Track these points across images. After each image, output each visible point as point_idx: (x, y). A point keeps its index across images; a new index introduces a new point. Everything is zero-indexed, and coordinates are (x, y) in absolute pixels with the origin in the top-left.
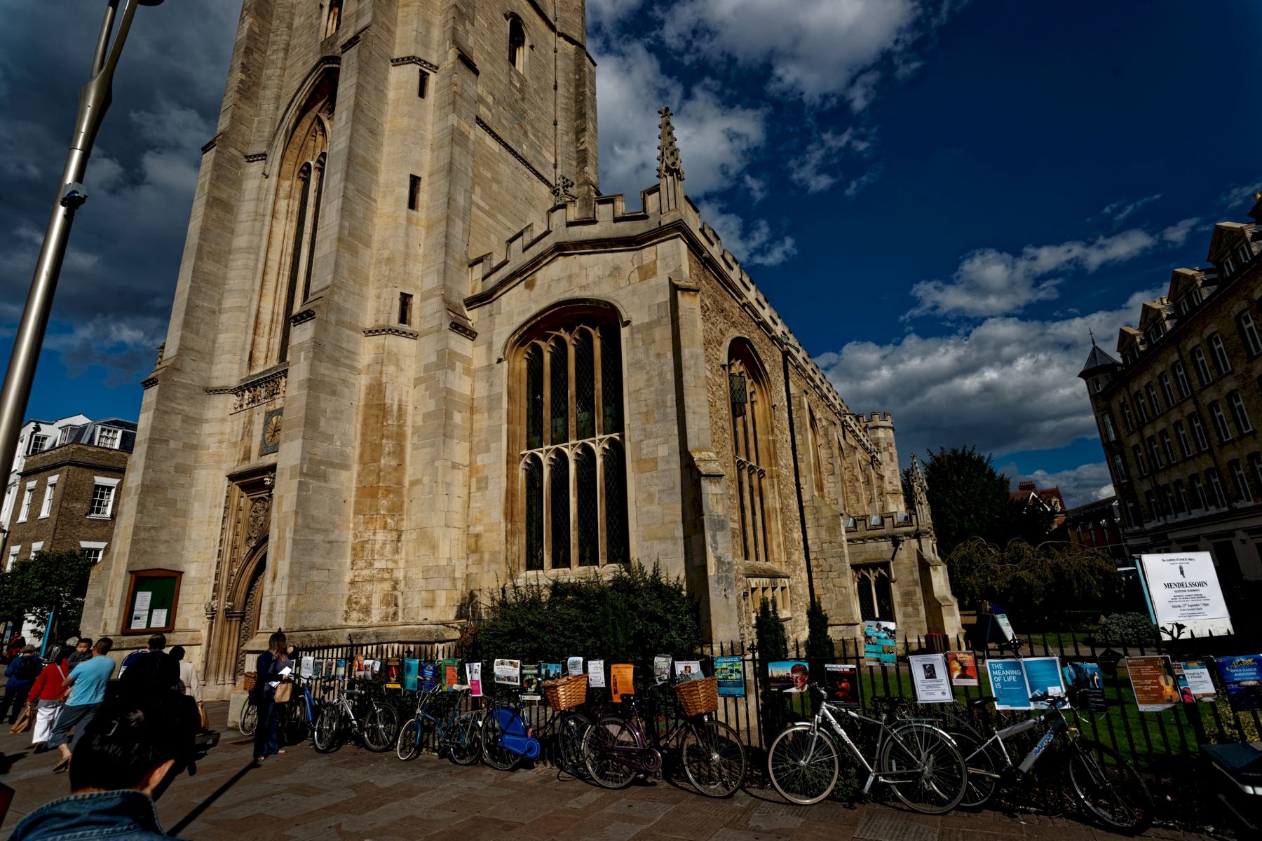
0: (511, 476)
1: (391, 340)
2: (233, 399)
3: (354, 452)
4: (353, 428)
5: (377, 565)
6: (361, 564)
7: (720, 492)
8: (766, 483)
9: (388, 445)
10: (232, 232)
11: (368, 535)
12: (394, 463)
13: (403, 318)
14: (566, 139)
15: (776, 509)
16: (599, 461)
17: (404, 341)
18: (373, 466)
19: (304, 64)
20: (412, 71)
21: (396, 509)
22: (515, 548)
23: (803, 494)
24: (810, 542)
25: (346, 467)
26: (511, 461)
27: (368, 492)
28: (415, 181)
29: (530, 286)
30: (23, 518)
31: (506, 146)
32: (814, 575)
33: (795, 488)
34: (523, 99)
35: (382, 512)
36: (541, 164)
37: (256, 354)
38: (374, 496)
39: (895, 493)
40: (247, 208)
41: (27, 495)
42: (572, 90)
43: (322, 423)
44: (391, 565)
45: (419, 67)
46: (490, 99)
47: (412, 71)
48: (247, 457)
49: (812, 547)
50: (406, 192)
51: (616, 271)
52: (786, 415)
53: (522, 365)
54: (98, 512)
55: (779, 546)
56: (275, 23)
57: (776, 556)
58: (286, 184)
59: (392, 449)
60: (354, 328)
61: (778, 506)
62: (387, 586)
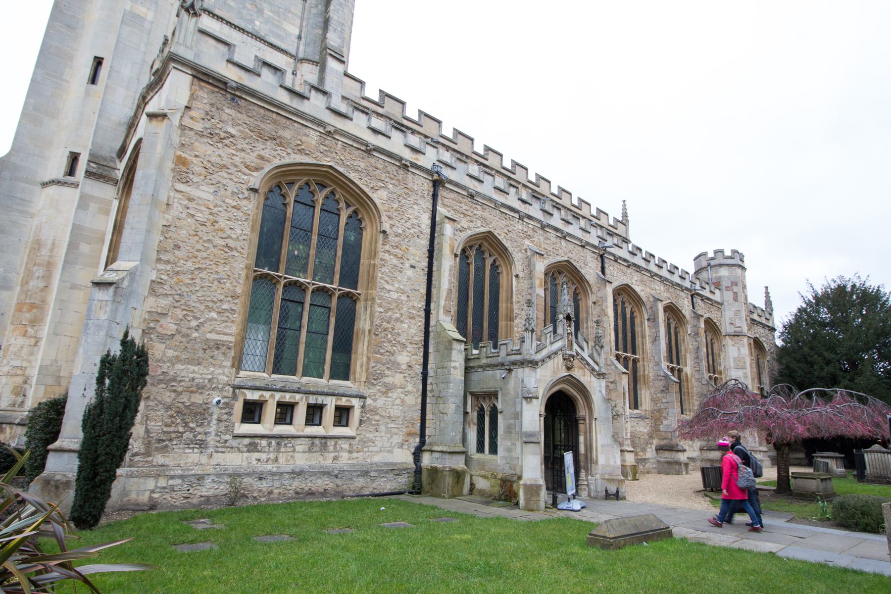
1: (53, 190)
4: (20, 259)
7: (106, 298)
8: (360, 306)
12: (41, 285)
13: (71, 171)
15: (364, 330)
21: (35, 322)
23: (431, 319)
24: (429, 367)
31: (228, 23)
32: (428, 400)
33: (423, 314)
35: (24, 323)
36: (278, 36)
39: (737, 335)
44: (25, 364)
49: (431, 372)
50: (87, 71)
52: (425, 242)
55: (361, 366)
57: (358, 376)
59: (41, 274)
61: (367, 327)
62: (19, 380)
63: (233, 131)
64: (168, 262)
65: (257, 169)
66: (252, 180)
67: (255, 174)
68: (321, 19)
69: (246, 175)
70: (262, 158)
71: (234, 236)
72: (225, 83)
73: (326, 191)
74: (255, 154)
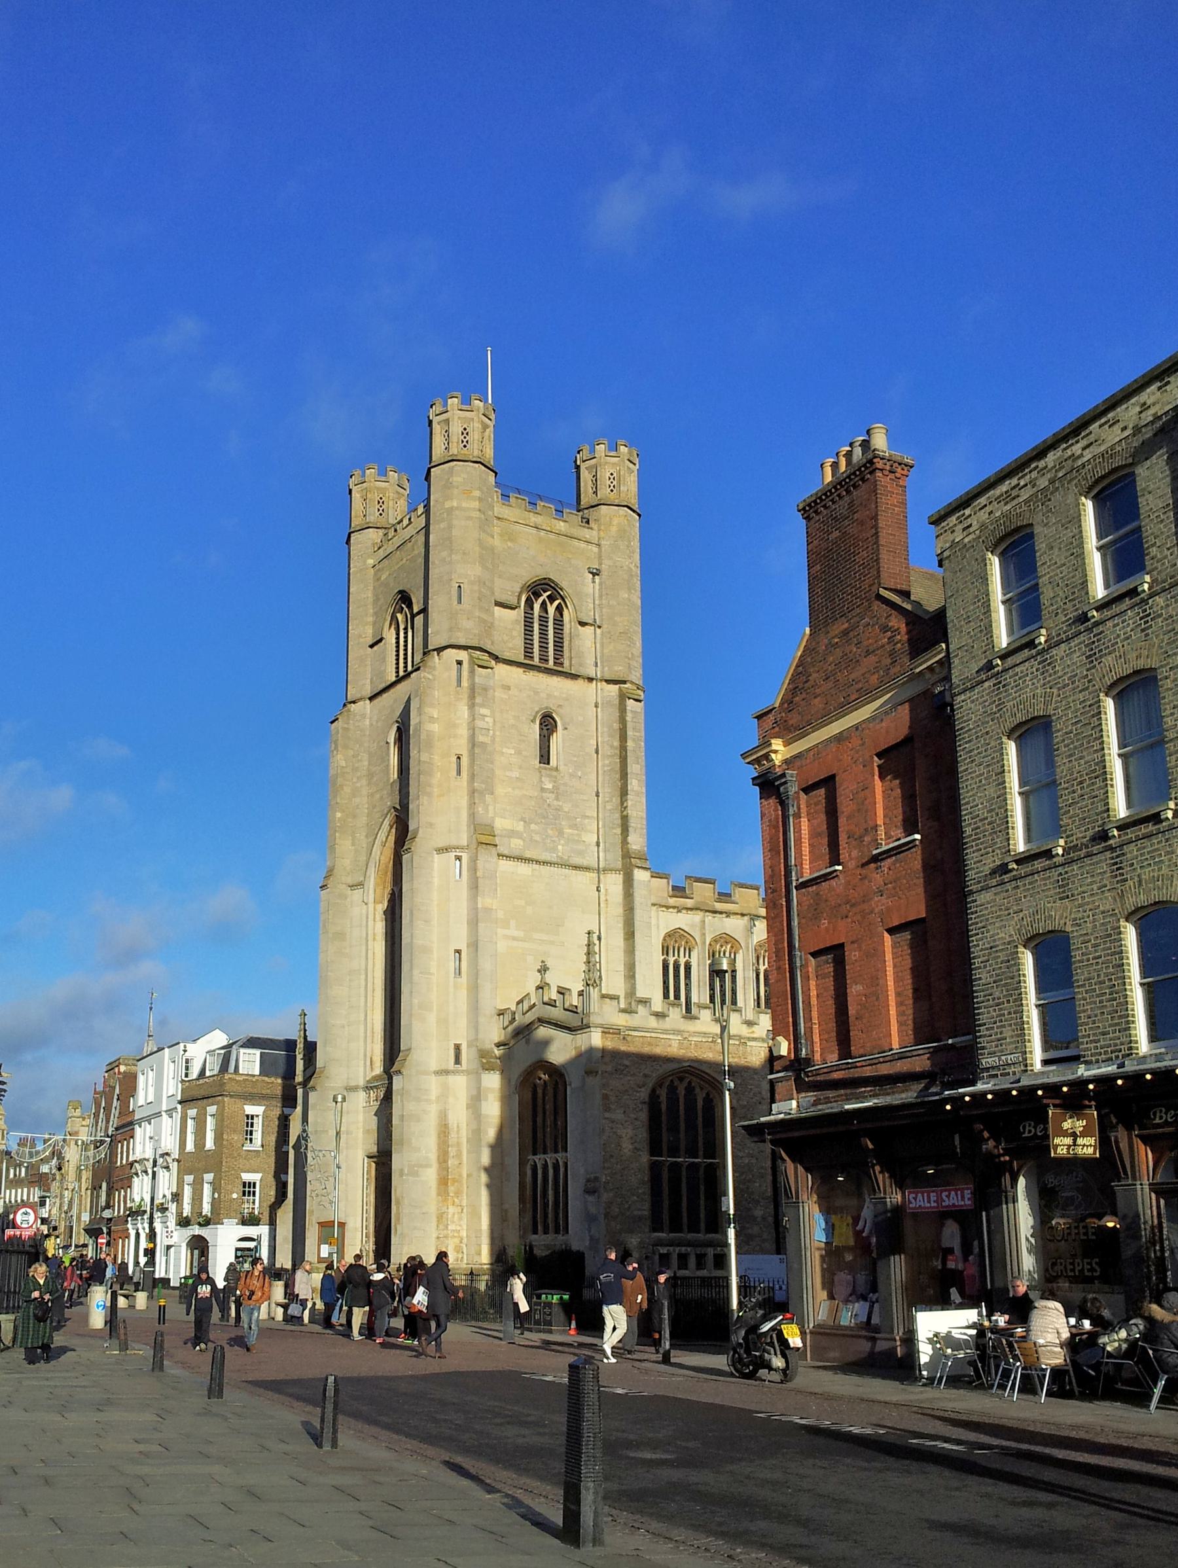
0: (522, 1174)
3: (434, 1156)
5: (449, 1228)
6: (441, 1227)
9: (452, 1151)
11: (444, 1209)
12: (457, 1163)
13: (458, 1061)
16: (562, 1170)
18: (444, 1165)
19: (381, 798)
22: (526, 1220)
25: (428, 1166)
26: (522, 1163)
27: (443, 1182)
29: (528, 1042)
34: (557, 799)
36: (581, 853)
37: (375, 1059)
38: (446, 1184)
43: (413, 1141)
44: (459, 1228)
46: (520, 827)
53: (528, 1096)
60: (426, 1073)
62: (457, 1241)
64: (608, 1168)
65: (644, 1086)
66: (642, 1094)
67: (643, 1089)
68: (617, 815)
69: (637, 1092)
70: (645, 1076)
73: (685, 1084)
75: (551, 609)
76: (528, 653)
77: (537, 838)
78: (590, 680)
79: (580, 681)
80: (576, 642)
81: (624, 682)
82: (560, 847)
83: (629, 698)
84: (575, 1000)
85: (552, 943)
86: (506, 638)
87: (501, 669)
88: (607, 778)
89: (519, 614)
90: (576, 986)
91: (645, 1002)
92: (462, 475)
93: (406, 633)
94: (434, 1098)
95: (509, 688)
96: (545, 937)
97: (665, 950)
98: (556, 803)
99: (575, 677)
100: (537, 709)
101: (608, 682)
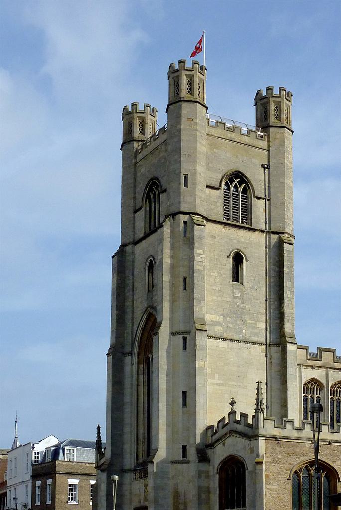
1: (180, 466)
2: (133, 475)
10: (123, 394)
13: (184, 455)
14: (273, 307)
17: (185, 465)
20: (181, 337)
28: (185, 393)
29: (224, 445)
30: (38, 503)
36: (256, 334)
40: (127, 382)
41: (38, 491)
42: (277, 270)
45: (183, 335)
46: (221, 319)
47: (181, 337)
48: (139, 502)
51: (245, 448)
54: (72, 499)
56: (127, 272)
58: (141, 366)
63: (280, 457)
70: (290, 464)
71: (286, 500)
72: (276, 438)
74: (287, 464)
75: (241, 190)
76: (227, 214)
77: (231, 326)
78: (263, 231)
79: (257, 232)
80: (254, 209)
81: (283, 233)
82: (244, 331)
83: (285, 243)
84: (250, 421)
85: (239, 387)
86: (213, 207)
87: (210, 226)
88: (272, 290)
89: (220, 193)
90: (251, 412)
91: (292, 422)
92: (187, 110)
93: (155, 204)
94: (171, 477)
95: (215, 237)
96: (236, 384)
97: (305, 391)
98: (242, 305)
99: (254, 230)
100: (231, 250)
101: (274, 233)
